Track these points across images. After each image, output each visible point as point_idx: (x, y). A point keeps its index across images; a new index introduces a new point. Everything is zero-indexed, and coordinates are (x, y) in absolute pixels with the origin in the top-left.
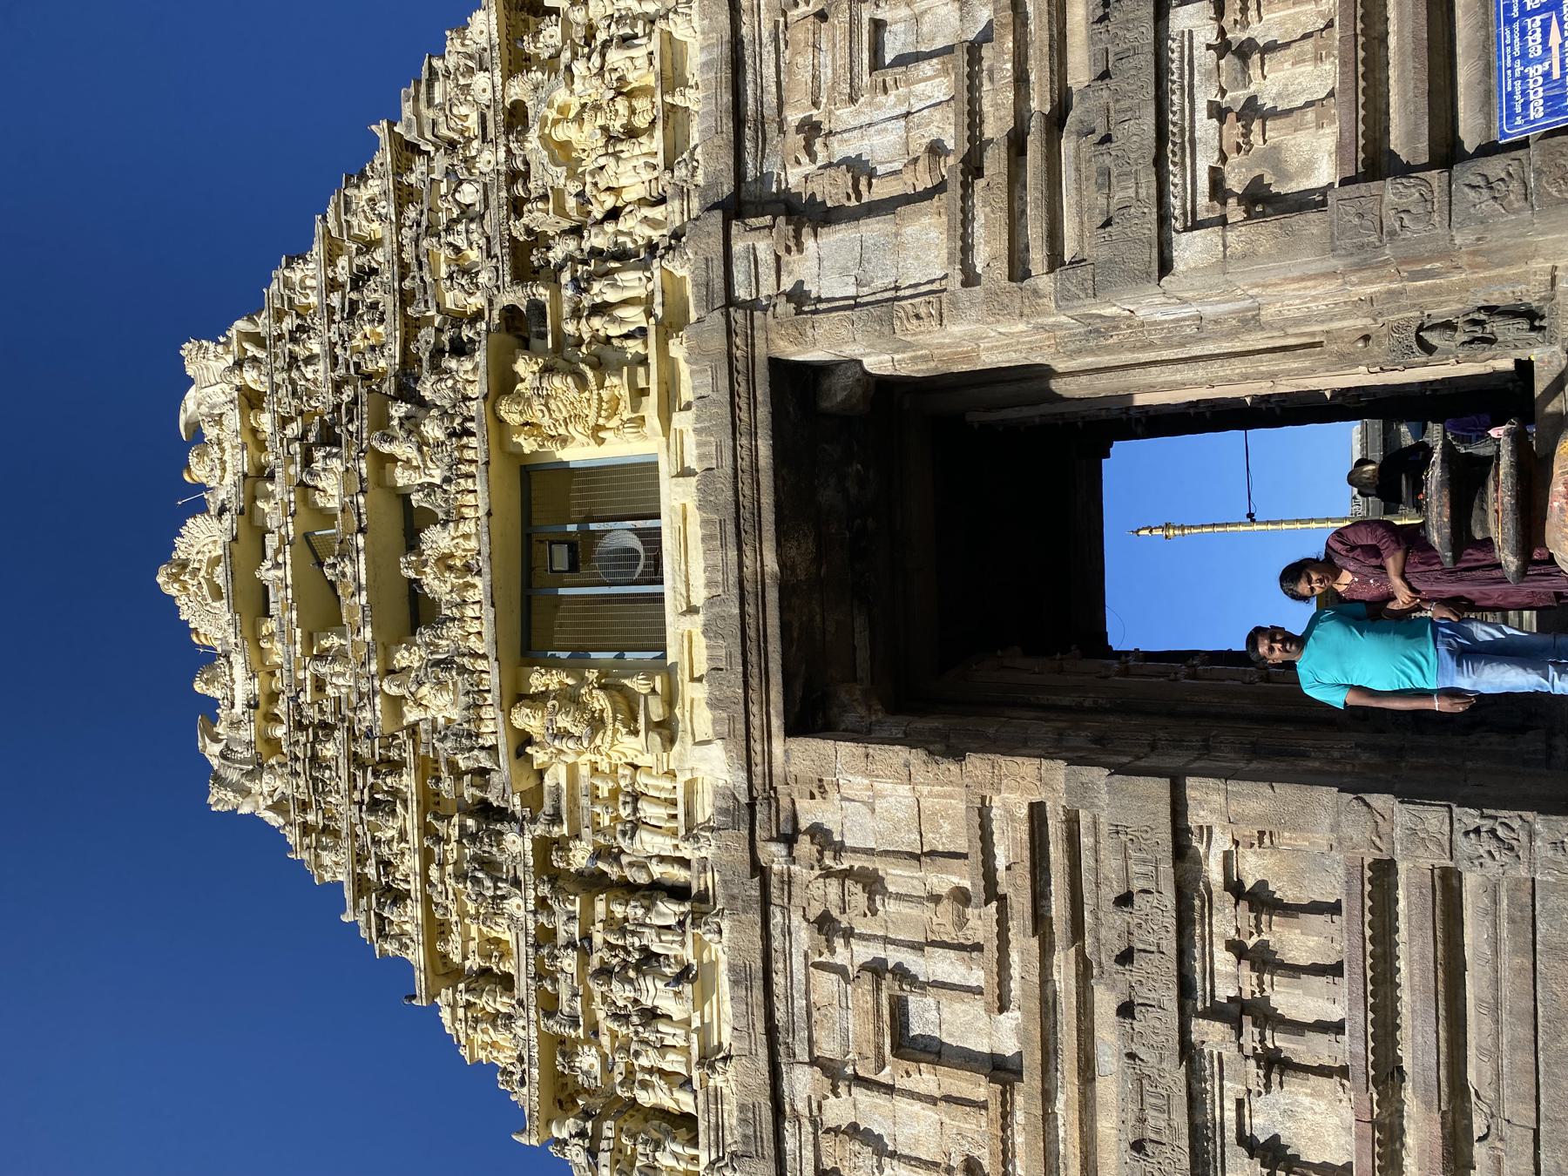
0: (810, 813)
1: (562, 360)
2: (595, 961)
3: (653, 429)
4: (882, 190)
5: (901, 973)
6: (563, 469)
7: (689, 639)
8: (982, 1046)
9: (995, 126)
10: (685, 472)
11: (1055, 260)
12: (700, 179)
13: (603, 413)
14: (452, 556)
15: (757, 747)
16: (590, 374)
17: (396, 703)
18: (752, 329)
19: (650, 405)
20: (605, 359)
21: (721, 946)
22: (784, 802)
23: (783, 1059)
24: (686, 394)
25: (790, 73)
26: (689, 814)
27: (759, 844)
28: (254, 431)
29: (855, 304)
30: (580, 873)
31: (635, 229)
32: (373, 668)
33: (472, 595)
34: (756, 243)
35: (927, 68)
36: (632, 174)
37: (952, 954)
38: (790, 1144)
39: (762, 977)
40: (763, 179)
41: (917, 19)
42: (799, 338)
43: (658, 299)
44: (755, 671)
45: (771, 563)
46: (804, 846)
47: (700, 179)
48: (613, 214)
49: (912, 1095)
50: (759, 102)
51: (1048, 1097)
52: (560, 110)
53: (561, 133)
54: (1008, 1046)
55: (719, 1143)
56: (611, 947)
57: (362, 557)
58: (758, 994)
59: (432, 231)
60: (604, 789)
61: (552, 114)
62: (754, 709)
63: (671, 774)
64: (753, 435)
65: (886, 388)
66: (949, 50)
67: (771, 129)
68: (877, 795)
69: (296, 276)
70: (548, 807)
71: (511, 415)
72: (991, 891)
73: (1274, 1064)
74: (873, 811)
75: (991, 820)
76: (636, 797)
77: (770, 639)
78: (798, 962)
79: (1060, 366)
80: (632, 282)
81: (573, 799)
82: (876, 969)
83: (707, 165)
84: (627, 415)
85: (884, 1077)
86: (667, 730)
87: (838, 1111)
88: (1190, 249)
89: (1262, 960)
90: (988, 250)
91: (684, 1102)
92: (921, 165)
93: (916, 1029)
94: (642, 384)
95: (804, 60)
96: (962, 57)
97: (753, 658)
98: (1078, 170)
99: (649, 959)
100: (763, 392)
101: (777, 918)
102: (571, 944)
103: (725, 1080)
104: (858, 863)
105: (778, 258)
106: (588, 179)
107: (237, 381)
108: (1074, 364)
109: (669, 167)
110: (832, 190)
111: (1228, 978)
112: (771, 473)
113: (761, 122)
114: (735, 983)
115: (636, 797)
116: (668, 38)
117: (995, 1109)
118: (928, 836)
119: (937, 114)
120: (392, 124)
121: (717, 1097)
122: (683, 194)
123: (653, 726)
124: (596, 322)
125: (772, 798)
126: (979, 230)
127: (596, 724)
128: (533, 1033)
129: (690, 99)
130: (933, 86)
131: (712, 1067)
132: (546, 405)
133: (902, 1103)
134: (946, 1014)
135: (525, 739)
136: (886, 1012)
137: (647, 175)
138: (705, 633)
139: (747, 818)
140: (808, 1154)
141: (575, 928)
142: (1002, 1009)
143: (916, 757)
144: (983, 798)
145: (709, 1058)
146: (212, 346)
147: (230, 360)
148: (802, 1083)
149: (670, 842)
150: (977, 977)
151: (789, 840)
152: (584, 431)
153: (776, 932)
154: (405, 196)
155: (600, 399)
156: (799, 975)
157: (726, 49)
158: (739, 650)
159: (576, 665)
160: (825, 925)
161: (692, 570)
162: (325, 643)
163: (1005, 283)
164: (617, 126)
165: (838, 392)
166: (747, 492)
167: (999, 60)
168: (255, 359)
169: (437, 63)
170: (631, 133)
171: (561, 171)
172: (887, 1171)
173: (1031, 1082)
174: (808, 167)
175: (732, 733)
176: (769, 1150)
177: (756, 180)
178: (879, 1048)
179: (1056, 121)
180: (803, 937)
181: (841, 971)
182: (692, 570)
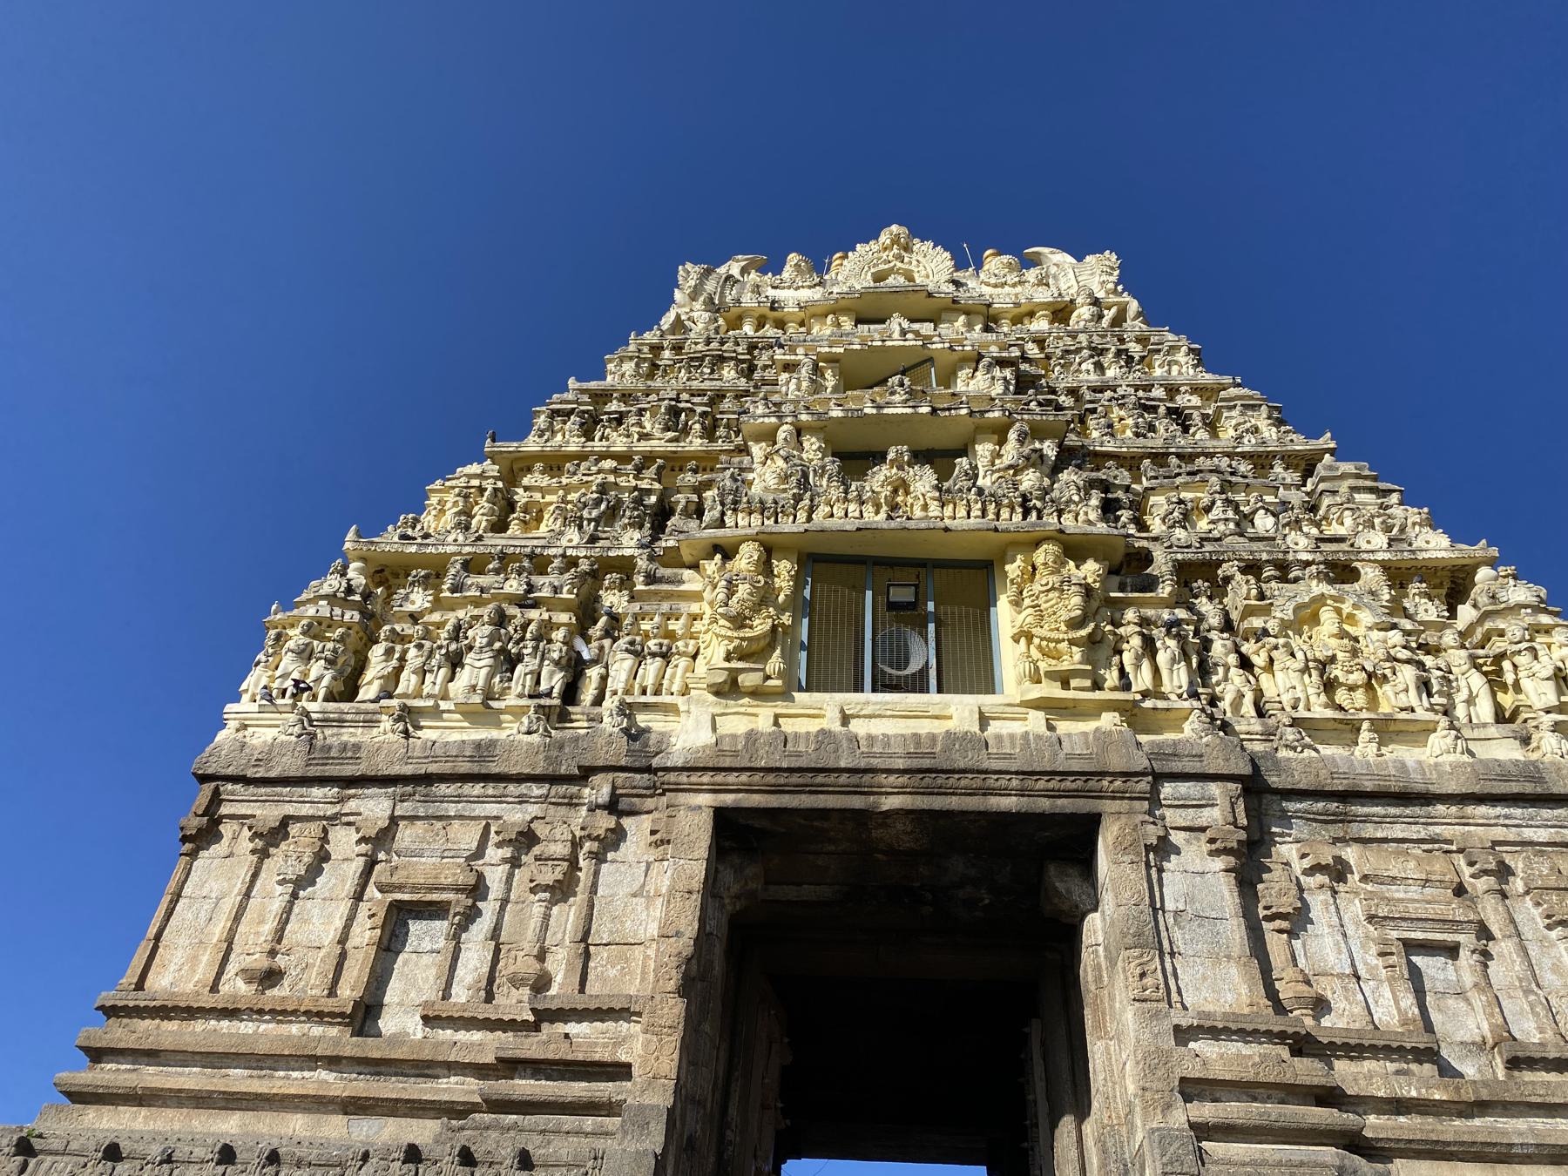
1: (1097, 606)
2: (513, 610)
3: (1028, 691)
4: (1276, 944)
5: (471, 915)
6: (989, 601)
7: (817, 714)
8: (391, 996)
9: (1349, 1074)
10: (984, 721)
11: (1203, 1131)
12: (1283, 753)
13: (1044, 643)
14: (907, 493)
15: (706, 778)
16: (1083, 633)
17: (769, 436)
18: (1130, 799)
19: (1054, 690)
20: (1100, 648)
21: (516, 734)
22: (650, 803)
23: (399, 790)
24: (1064, 727)
25: (1398, 853)
26: (646, 707)
27: (611, 776)
28: (1031, 314)
29: (1156, 909)
30: (597, 599)
32: (804, 417)
33: (868, 510)
34: (1218, 808)
35: (1408, 1001)
36: (1285, 684)
37: (486, 969)
38: (317, 792)
39: (482, 772)
40: (1285, 819)
41: (1461, 994)
42: (1121, 847)
43: (1161, 704)
44: (782, 781)
45: (891, 803)
46: (605, 822)
47: (1283, 753)
48: (1245, 664)
49: (351, 919)
50: (1366, 819)
51: (333, 1062)
52: (1351, 616)
53: (1326, 615)
54: (388, 1024)
55: (326, 722)
56: (525, 627)
57: (909, 411)
58: (464, 767)
59: (1227, 486)
60: (676, 626)
61: (1347, 608)
62: (744, 777)
63: (685, 691)
64: (1022, 793)
65: (1069, 935)
66: (1429, 1027)
67: (1337, 830)
68: (650, 900)
69: (1181, 356)
70: (663, 572)
72: (546, 1016)
74: (634, 895)
75: (616, 1021)
76: (666, 656)
77: (813, 797)
78: (491, 809)
79: (1088, 1128)
80: (1177, 678)
81: (669, 596)
82: (477, 889)
83: (1299, 762)
84: (1043, 666)
85: (372, 891)
86: (728, 689)
87: (344, 842)
90: (1214, 1057)
91: (368, 691)
92: (1303, 988)
93: (415, 927)
94: (1074, 683)
95: (1411, 869)
96: (1421, 1041)
97: (795, 779)
98: (1302, 1164)
99: (508, 662)
100: (1065, 805)
101: (536, 790)
102: (531, 588)
103: (386, 731)
105: (1203, 829)
106: (1281, 641)
107: (1079, 300)
108: (1089, 1142)
109: (1295, 723)
110: (1274, 891)
112: (982, 808)
113: (1345, 819)
114: (478, 745)
115: (666, 656)
116: (1430, 729)
117: (329, 1005)
118: (604, 953)
119: (1358, 1010)
120: (1332, 452)
121: (370, 722)
122: (1268, 735)
123: (733, 675)
124: (1136, 641)
125: (655, 790)
126: (1235, 1047)
127: (739, 621)
128: (450, 549)
129: (1366, 748)
130: (1390, 1008)
131: (399, 719)
132: (1053, 589)
133: (344, 908)
134: (426, 959)
135: (727, 552)
136: (435, 897)
137: (1286, 699)
138: (822, 731)
139: (637, 764)
140: (306, 810)
141: (546, 593)
142: (426, 1020)
143: (685, 944)
144: (639, 1014)
145: (409, 717)
146: (1114, 278)
147: (1100, 295)
148: (374, 807)
149: (620, 687)
150: (460, 994)
151: (612, 807)
152: (1026, 623)
153: (523, 788)
154: (1261, 461)
155: (1058, 641)
156: (480, 810)
157: (1420, 788)
158: (804, 765)
159: (796, 603)
160: (526, 839)
161: (886, 723)
162: (828, 374)
163: (1180, 1072)
164: (1336, 671)
165: (1065, 884)
166: (963, 783)
167: (1418, 1083)
168: (1101, 317)
169: (1394, 498)
170: (1329, 686)
171: (1289, 615)
172: (280, 889)
173: (351, 1045)
174: (1298, 866)
175: (721, 753)
176: (314, 771)
177: (1284, 811)
178: (400, 888)
179: (1355, 1143)
180: (516, 816)
181: (479, 853)
182: (886, 723)
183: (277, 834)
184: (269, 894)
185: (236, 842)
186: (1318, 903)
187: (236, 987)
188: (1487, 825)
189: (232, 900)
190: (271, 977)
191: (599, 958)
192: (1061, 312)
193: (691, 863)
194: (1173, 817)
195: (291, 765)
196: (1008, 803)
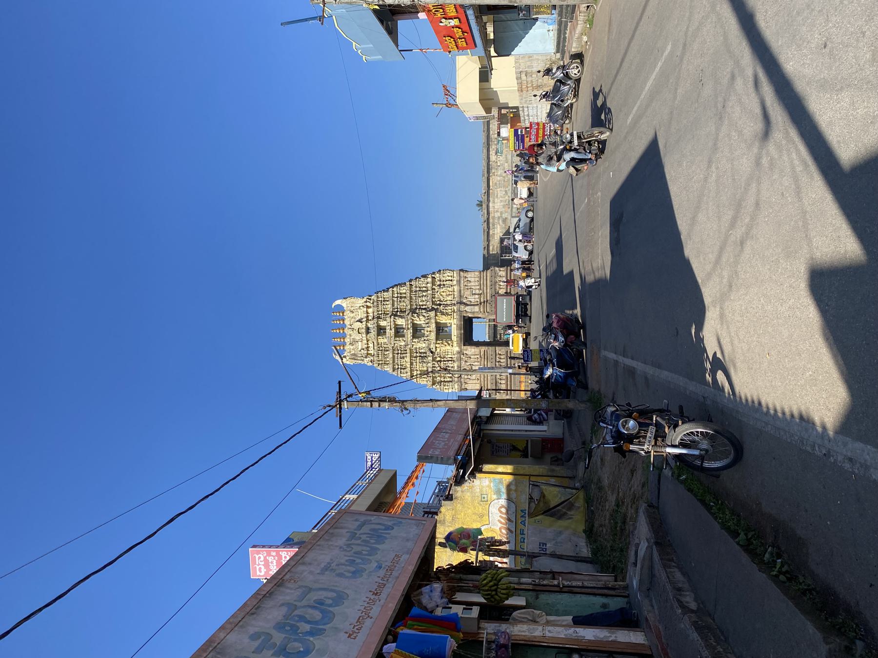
1: (443, 314)
7: (454, 338)
20: (447, 314)
31: (449, 303)
34: (462, 306)
36: (449, 298)
68: (471, 350)
111: (498, 360)
152: (443, 319)
154: (411, 291)
185: (467, 386)
188: (462, 285)
192: (368, 307)
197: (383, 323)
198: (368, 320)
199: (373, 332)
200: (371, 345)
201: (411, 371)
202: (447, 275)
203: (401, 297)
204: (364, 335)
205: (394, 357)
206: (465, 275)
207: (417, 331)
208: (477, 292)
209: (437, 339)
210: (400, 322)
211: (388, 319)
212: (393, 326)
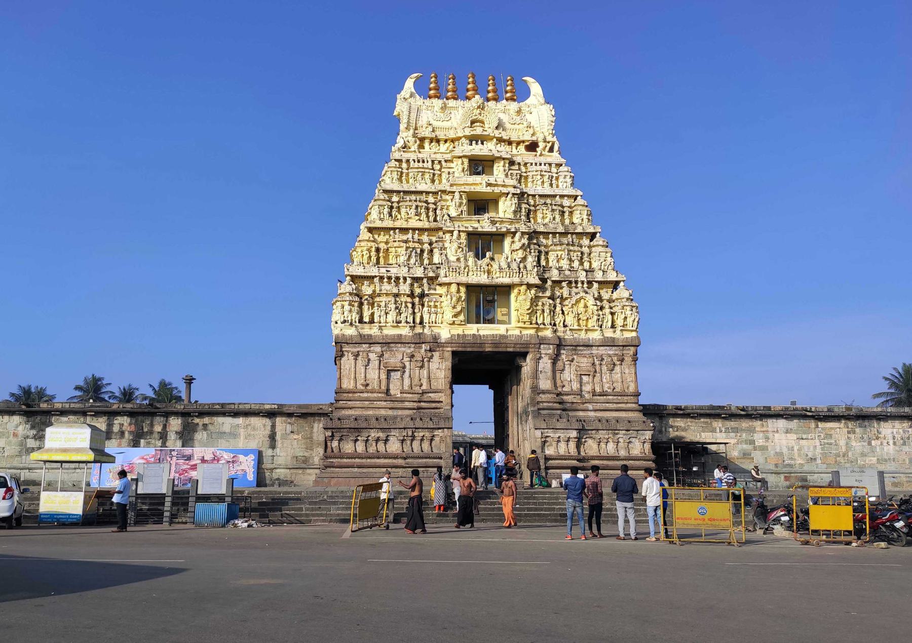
0: (436, 355)
1: (534, 301)
4: (558, 375)
5: (404, 372)
7: (473, 329)
9: (565, 397)
10: (507, 330)
11: (539, 409)
20: (532, 312)
21: (405, 331)
31: (559, 319)
34: (551, 350)
36: (570, 320)
38: (364, 346)
39: (399, 341)
45: (487, 350)
46: (429, 354)
48: (563, 313)
54: (392, 392)
68: (440, 368)
71: (523, 288)
73: (403, 441)
80: (547, 320)
82: (404, 367)
85: (382, 367)
87: (372, 356)
88: (538, 433)
89: (422, 440)
91: (366, 319)
100: (523, 350)
104: (426, 364)
110: (559, 364)
122: (564, 332)
127: (454, 307)
130: (576, 386)
133: (377, 371)
145: (380, 328)
148: (378, 349)
151: (430, 350)
152: (519, 302)
161: (486, 330)
167: (577, 399)
170: (579, 320)
182: (486, 330)
183: (356, 355)
184: (361, 369)
186: (567, 367)
187: (360, 387)
188: (602, 351)
189: (353, 369)
190: (367, 385)
191: (432, 381)
193: (448, 364)
194: (543, 352)
195: (358, 340)
196: (511, 350)
197: (499, 169)
198: (500, 140)
199: (478, 150)
200: (443, 147)
201: (387, 230)
202: (627, 317)
203: (562, 213)
204: (468, 132)
205: (421, 193)
206: (628, 360)
207: (482, 244)
208: (587, 388)
209: (470, 287)
210: (506, 208)
211: (510, 182)
212: (497, 190)
